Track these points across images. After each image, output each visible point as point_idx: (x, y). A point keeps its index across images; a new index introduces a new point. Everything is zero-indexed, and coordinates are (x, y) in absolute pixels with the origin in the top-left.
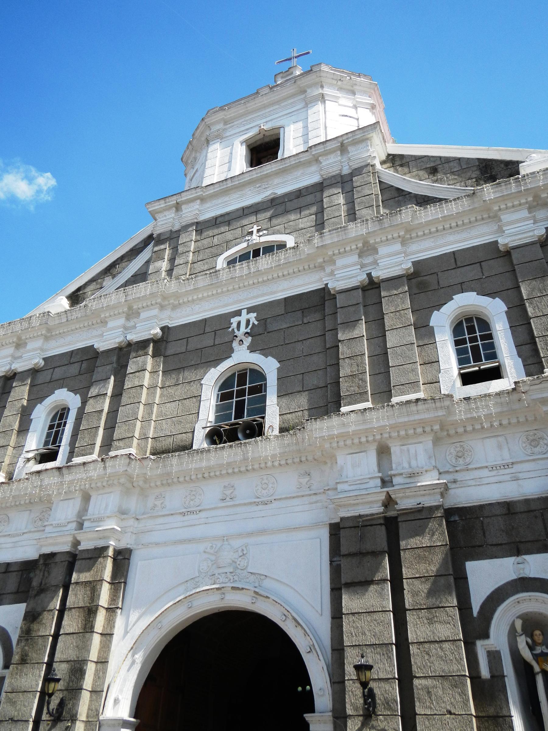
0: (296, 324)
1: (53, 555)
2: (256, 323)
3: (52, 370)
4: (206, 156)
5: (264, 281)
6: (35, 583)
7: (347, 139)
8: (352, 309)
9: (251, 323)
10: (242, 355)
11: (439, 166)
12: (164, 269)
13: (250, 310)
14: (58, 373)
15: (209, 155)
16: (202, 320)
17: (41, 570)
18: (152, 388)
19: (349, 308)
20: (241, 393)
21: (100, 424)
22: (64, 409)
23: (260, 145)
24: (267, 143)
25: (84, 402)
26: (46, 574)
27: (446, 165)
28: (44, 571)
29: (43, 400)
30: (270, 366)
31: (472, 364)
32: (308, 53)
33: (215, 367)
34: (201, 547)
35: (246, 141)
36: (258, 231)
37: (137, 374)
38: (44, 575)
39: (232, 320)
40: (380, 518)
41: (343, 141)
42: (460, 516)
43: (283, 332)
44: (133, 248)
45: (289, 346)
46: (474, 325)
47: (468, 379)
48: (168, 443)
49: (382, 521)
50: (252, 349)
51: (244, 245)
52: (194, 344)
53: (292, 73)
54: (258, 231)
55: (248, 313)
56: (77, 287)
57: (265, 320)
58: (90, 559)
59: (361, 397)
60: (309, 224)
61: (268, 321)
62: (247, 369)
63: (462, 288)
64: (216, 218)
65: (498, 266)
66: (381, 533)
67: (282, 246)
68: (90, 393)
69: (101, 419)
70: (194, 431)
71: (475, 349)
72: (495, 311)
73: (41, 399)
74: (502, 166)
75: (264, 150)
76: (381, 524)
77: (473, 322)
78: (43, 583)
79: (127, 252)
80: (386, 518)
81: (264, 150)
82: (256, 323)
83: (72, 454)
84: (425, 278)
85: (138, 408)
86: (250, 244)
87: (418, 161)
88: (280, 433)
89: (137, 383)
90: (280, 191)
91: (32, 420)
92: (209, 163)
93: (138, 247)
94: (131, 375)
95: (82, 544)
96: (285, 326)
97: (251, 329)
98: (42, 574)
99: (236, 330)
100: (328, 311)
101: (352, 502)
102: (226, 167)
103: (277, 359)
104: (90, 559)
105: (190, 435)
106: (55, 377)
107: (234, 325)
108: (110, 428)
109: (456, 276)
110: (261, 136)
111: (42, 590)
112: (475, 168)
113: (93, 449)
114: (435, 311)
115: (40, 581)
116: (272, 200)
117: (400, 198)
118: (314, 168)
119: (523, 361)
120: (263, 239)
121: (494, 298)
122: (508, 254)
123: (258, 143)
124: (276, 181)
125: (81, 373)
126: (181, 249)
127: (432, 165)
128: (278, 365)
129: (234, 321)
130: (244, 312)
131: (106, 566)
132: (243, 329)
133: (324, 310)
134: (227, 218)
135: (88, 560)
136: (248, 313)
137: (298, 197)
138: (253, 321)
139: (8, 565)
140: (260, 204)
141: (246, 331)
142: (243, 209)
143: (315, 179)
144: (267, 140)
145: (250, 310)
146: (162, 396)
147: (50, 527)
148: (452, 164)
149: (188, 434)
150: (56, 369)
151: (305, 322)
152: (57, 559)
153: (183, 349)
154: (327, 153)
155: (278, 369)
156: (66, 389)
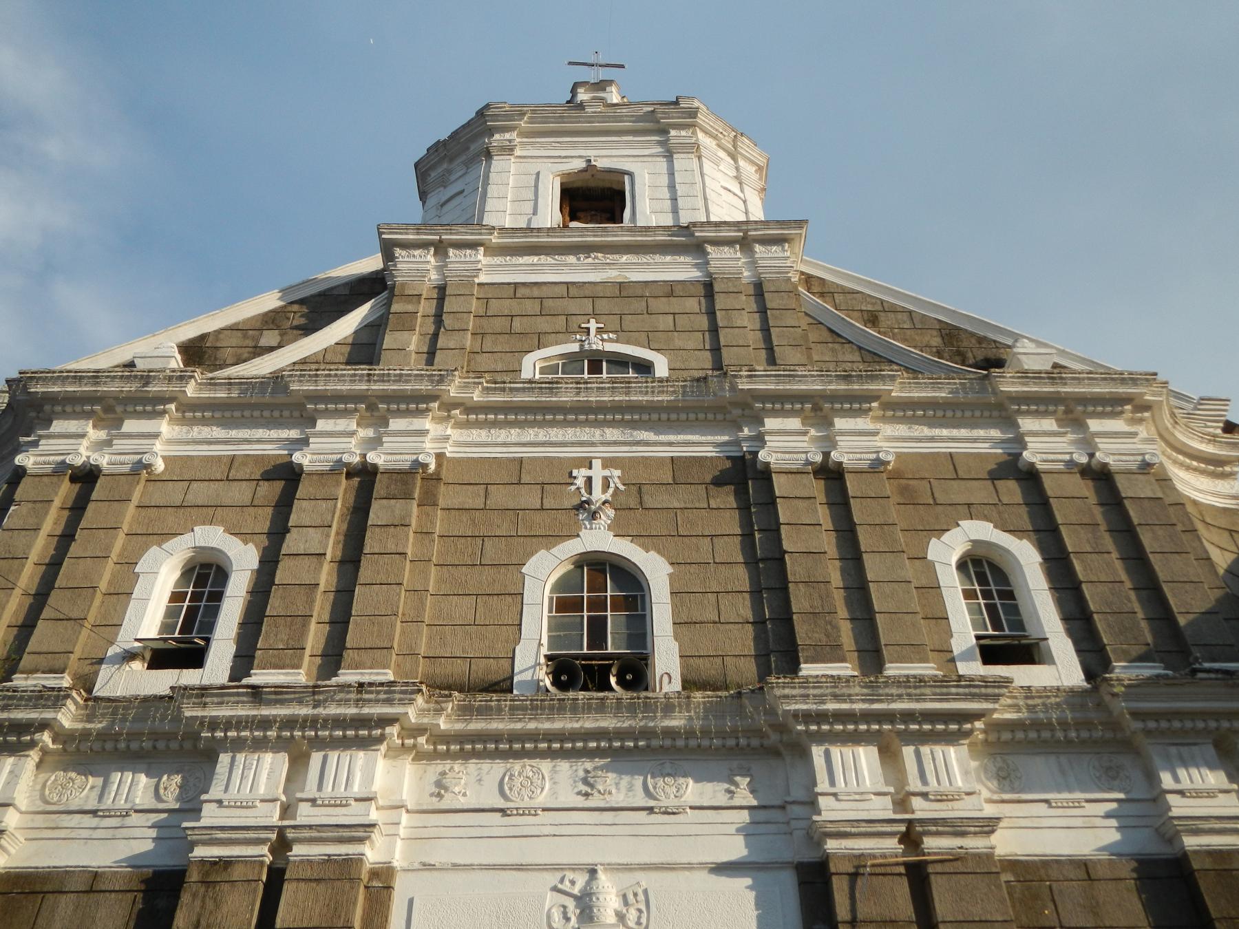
0: (697, 505)
2: (622, 487)
3: (187, 484)
4: (487, 177)
5: (632, 421)
7: (755, 230)
8: (801, 504)
9: (612, 485)
10: (598, 538)
11: (882, 314)
12: (412, 347)
13: (608, 463)
14: (200, 493)
15: (493, 177)
16: (514, 459)
17: (194, 896)
18: (422, 561)
19: (796, 501)
20: (598, 604)
21: (311, 610)
22: (206, 566)
23: (578, 189)
24: (589, 189)
26: (210, 904)
27: (891, 315)
28: (204, 897)
29: (164, 541)
30: (656, 570)
31: (991, 632)
32: (622, 66)
33: (548, 549)
34: (552, 879)
35: (563, 175)
36: (600, 331)
37: (392, 529)
38: (203, 907)
39: (575, 473)
40: (897, 864)
41: (748, 230)
42: (1015, 874)
43: (673, 515)
44: (325, 291)
45: (686, 539)
46: (984, 574)
47: (991, 654)
48: (458, 670)
49: (902, 870)
50: (619, 530)
51: (575, 347)
52: (500, 497)
53: (604, 90)
55: (605, 467)
56: (199, 333)
57: (640, 487)
58: (318, 881)
59: (832, 653)
60: (691, 345)
61: (644, 489)
62: (604, 564)
63: (972, 510)
64: (516, 285)
66: (902, 890)
67: (644, 367)
68: (285, 546)
69: (313, 601)
70: (513, 658)
71: (991, 609)
72: (1026, 558)
73: (164, 536)
74: (973, 341)
75: (594, 199)
76: (900, 874)
77: (982, 566)
78: (203, 923)
79: (313, 296)
80: (905, 864)
81: (594, 199)
82: (622, 487)
83: (244, 661)
84: (911, 482)
85: (399, 595)
86: (587, 347)
87: (849, 296)
88: (684, 688)
89: (391, 547)
91: (138, 575)
92: (492, 190)
93: (335, 292)
94: (377, 529)
95: (294, 848)
96: (677, 505)
97: (613, 496)
98: (198, 903)
99: (583, 491)
101: (848, 829)
102: (528, 208)
103: (668, 559)
104: (318, 881)
105: (505, 664)
106: (191, 499)
107: (580, 482)
108: (340, 620)
109: (957, 493)
110: (587, 175)
112: (935, 333)
113: (301, 658)
114: (934, 540)
115: (195, 918)
117: (837, 346)
119: (1076, 643)
120: (610, 347)
121: (1021, 539)
123: (575, 185)
125: (255, 503)
126: (448, 321)
127: (870, 308)
128: (670, 569)
129: (581, 474)
130: (597, 464)
131: (356, 899)
132: (598, 495)
134: (536, 292)
135: (314, 885)
136: (605, 467)
137: (671, 294)
138: (616, 482)
139: (96, 875)
140: (599, 288)
141: (604, 498)
144: (592, 184)
145: (608, 463)
146: (440, 581)
147: (214, 805)
148: (900, 316)
149: (502, 661)
150: (195, 485)
151: (713, 505)
152: (237, 873)
153: (479, 503)
154: (717, 243)
155: (670, 575)
156: (222, 529)
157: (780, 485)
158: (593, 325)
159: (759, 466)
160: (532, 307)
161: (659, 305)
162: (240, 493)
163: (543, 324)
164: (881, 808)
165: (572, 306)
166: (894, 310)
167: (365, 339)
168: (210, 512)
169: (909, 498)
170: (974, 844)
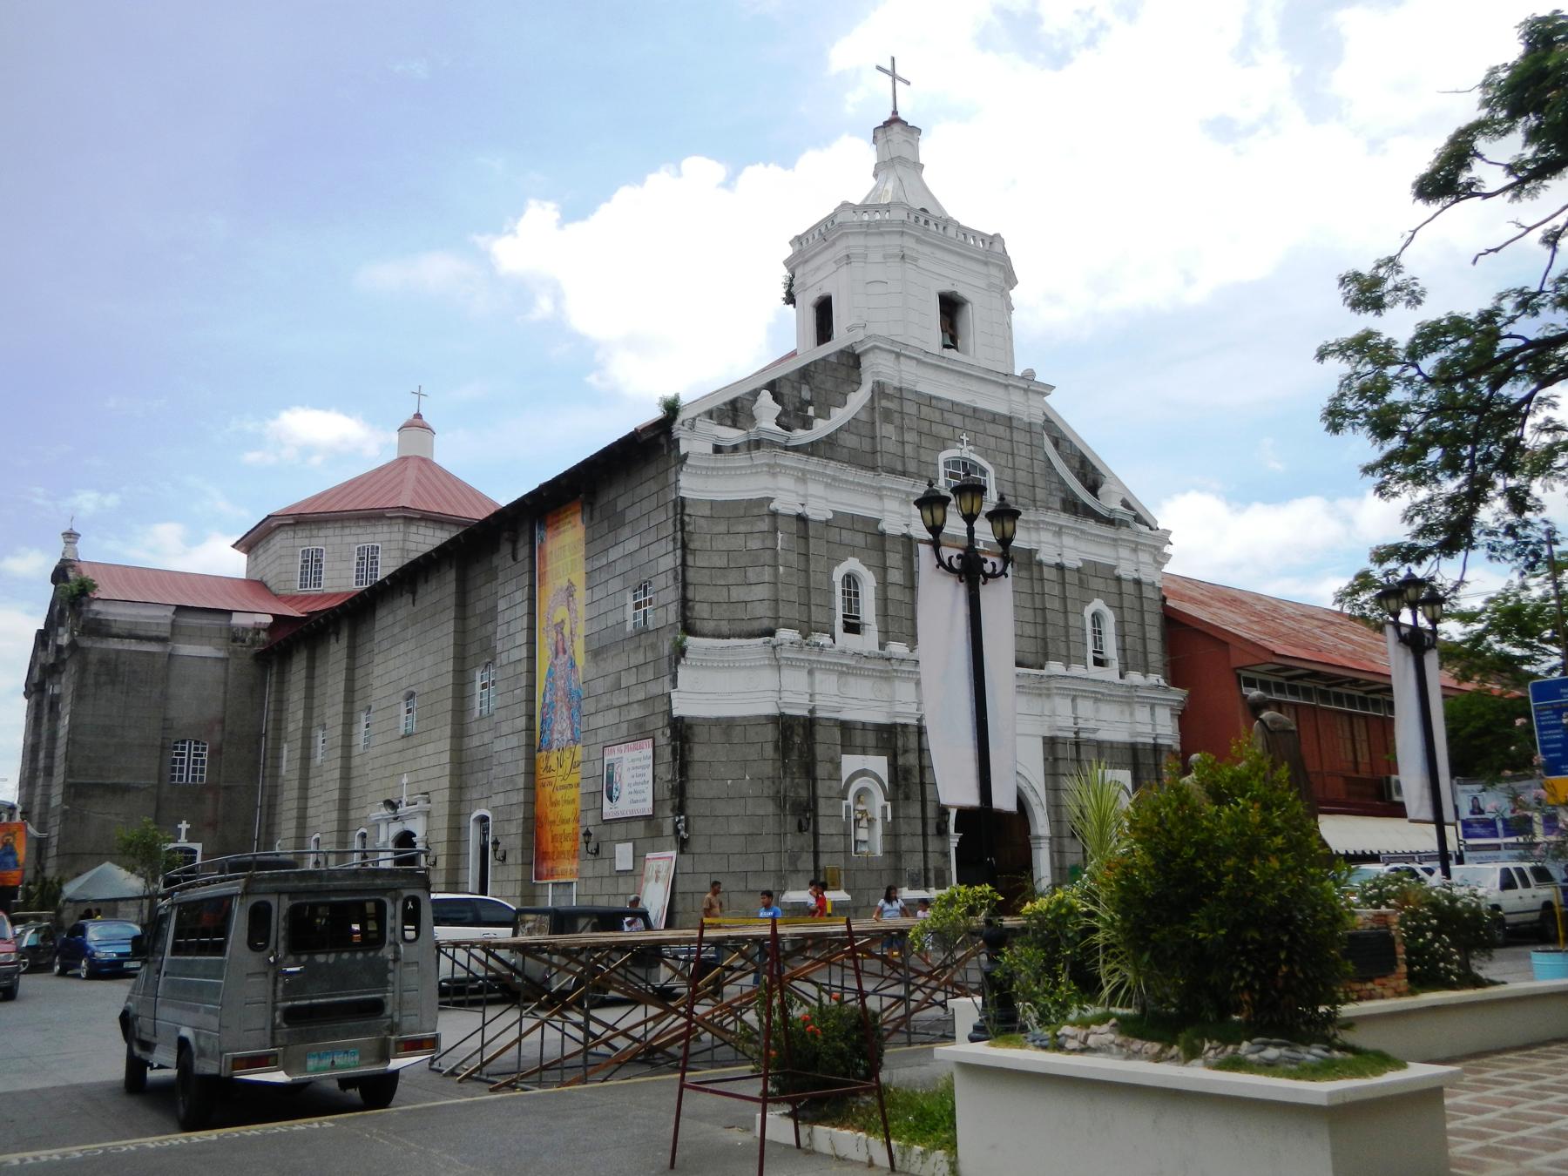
1: (905, 726)
6: (900, 743)
25: (883, 584)
54: (968, 443)
64: (931, 397)
65: (1113, 587)
72: (1110, 618)
73: (839, 562)
90: (981, 404)
100: (1036, 575)
111: (906, 751)
116: (975, 410)
118: (1000, 392)
122: (1119, 579)
124: (974, 386)
133: (1031, 570)
137: (993, 421)
142: (953, 403)
143: (1002, 408)
157: (1047, 574)
158: (964, 438)
159: (1038, 557)
160: (936, 416)
161: (990, 428)
162: (859, 540)
163: (945, 432)
164: (1070, 723)
165: (957, 420)
166: (1065, 439)
167: (864, 417)
168: (853, 551)
169: (1082, 584)
170: (1092, 736)
